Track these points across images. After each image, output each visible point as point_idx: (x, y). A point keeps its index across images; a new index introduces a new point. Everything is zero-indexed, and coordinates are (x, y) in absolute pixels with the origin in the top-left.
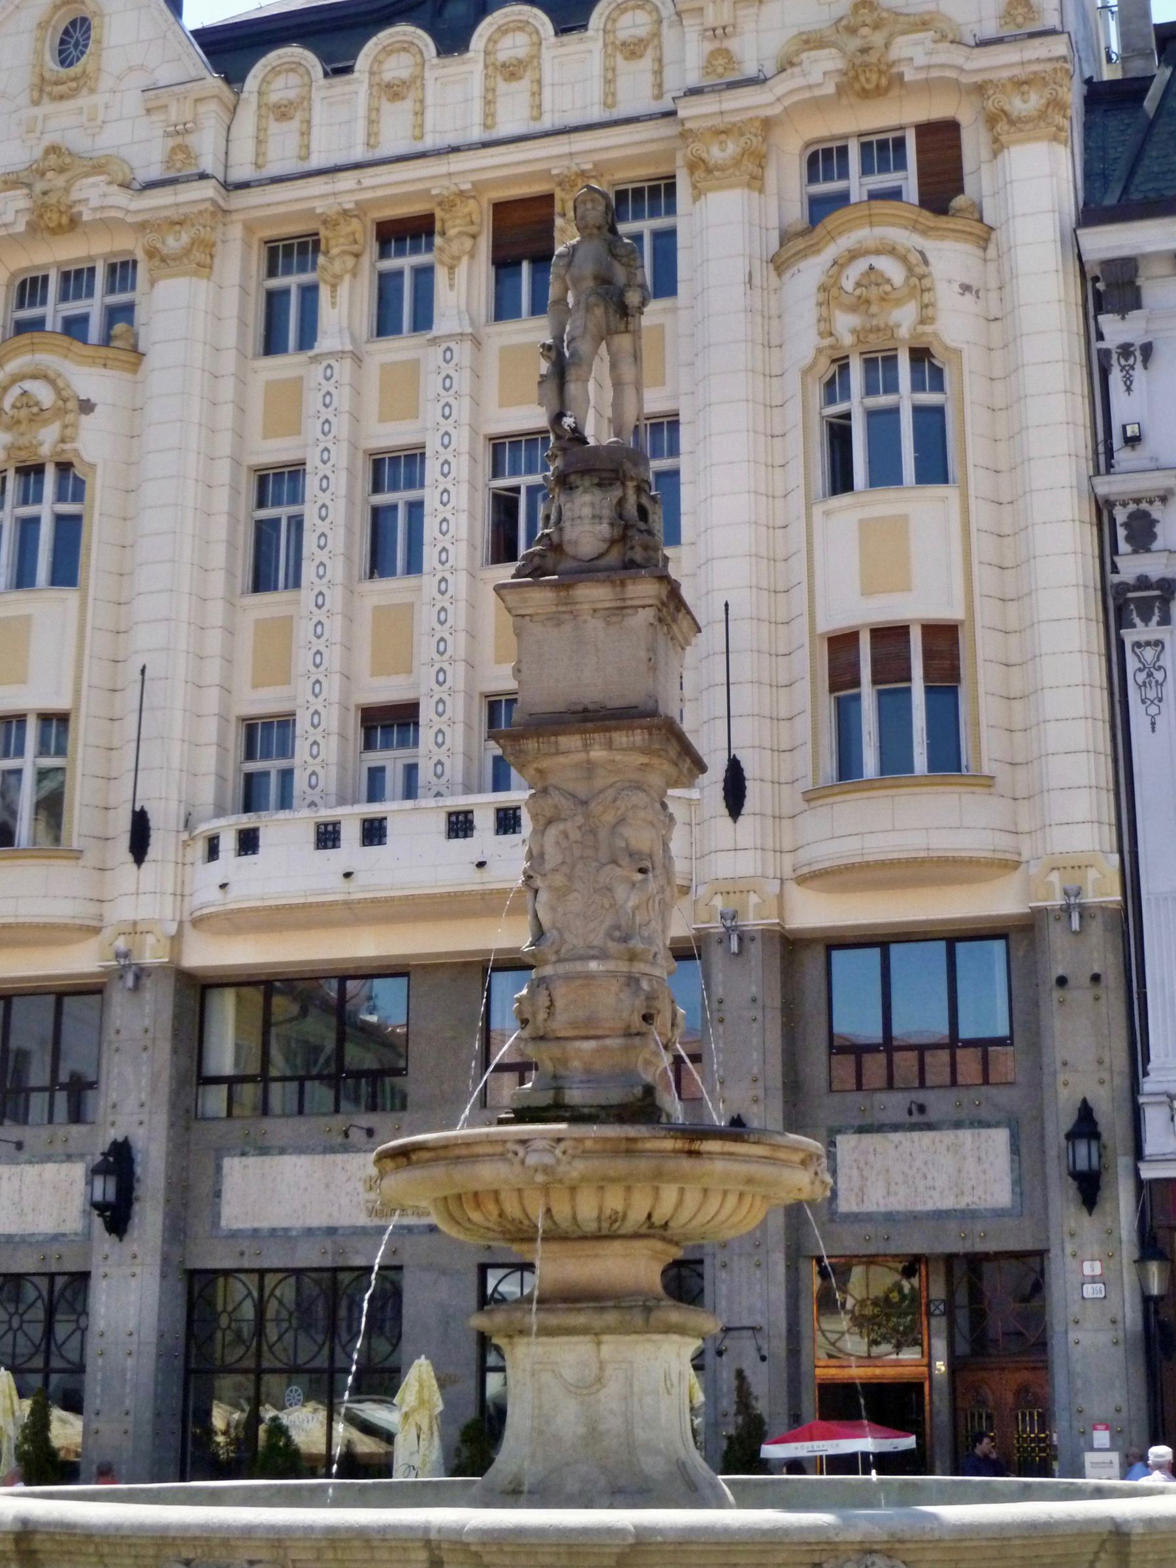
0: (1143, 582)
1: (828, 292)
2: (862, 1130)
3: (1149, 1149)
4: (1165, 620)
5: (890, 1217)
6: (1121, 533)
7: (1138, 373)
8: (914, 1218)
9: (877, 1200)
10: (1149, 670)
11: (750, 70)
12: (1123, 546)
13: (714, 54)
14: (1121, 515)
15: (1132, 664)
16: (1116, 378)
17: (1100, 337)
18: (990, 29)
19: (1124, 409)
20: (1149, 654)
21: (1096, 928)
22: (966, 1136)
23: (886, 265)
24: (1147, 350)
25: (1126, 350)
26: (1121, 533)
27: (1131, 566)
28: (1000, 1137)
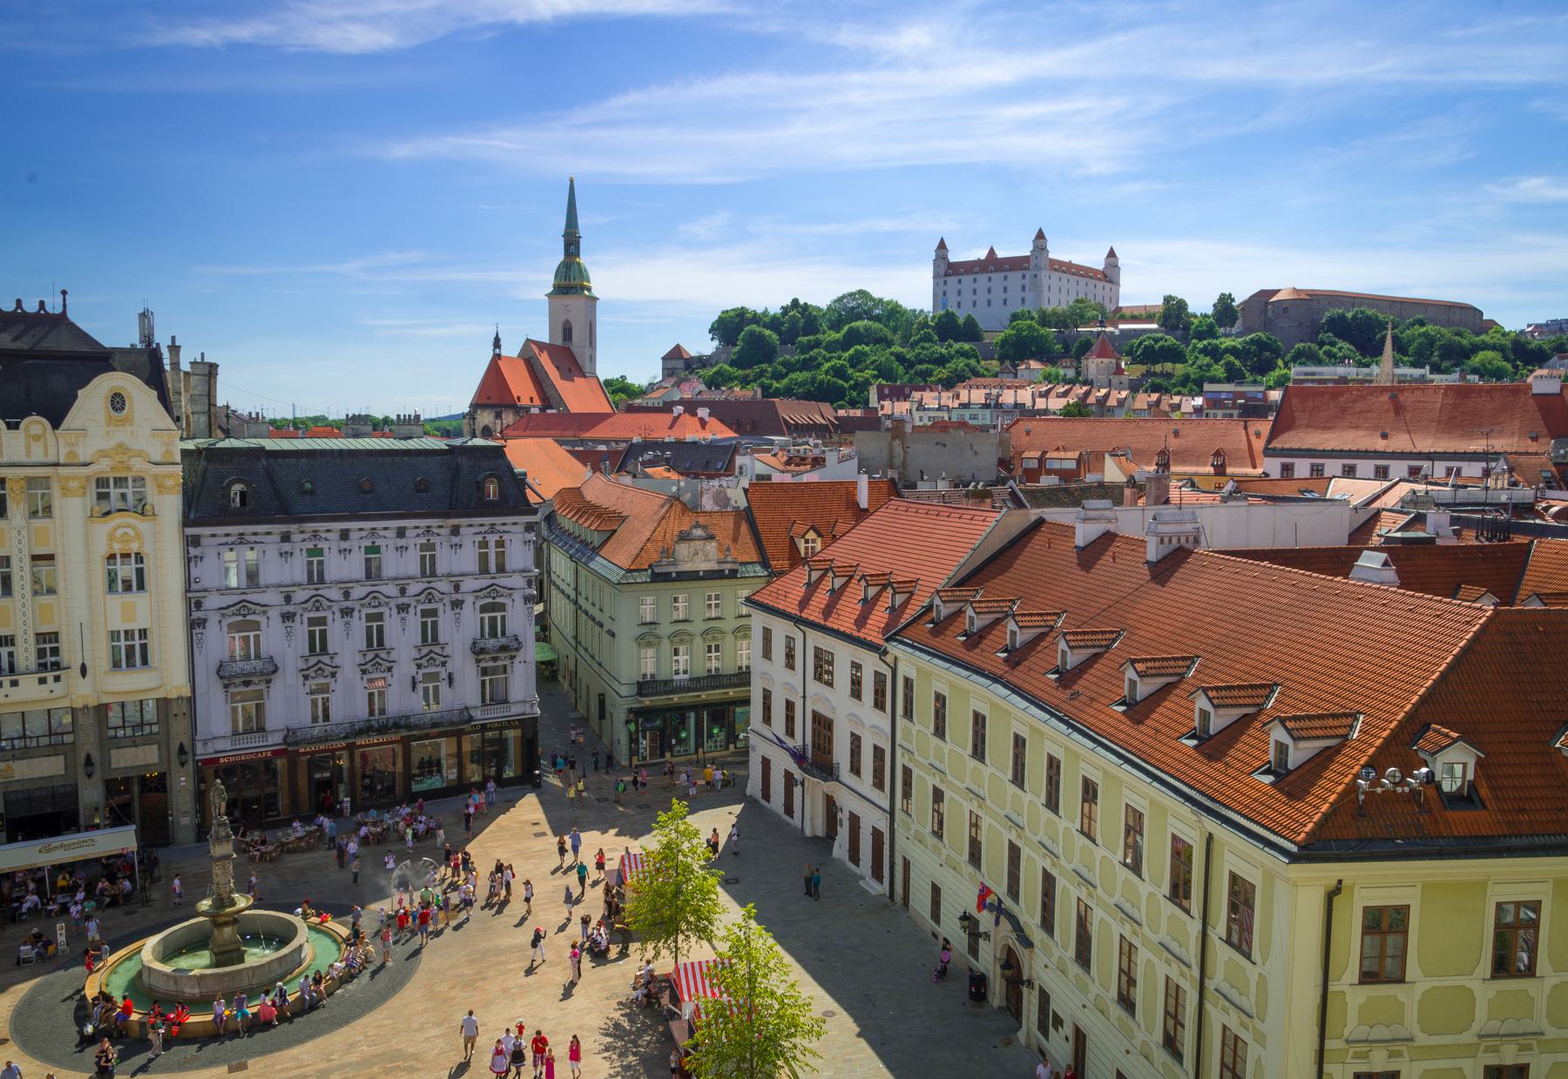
0: (199, 619)
1: (111, 537)
2: (118, 748)
3: (198, 752)
4: (204, 628)
5: (126, 768)
6: (193, 605)
7: (199, 563)
8: (132, 768)
9: (122, 764)
10: (199, 640)
11: (82, 459)
12: (193, 609)
13: (69, 453)
14: (193, 601)
15: (195, 638)
16: (192, 564)
17: (188, 553)
18: (158, 458)
19: (195, 572)
20: (200, 636)
21: (184, 701)
22: (146, 747)
23: (128, 530)
24: (202, 558)
25: (196, 557)
26: (193, 605)
27: (196, 615)
28: (156, 747)
